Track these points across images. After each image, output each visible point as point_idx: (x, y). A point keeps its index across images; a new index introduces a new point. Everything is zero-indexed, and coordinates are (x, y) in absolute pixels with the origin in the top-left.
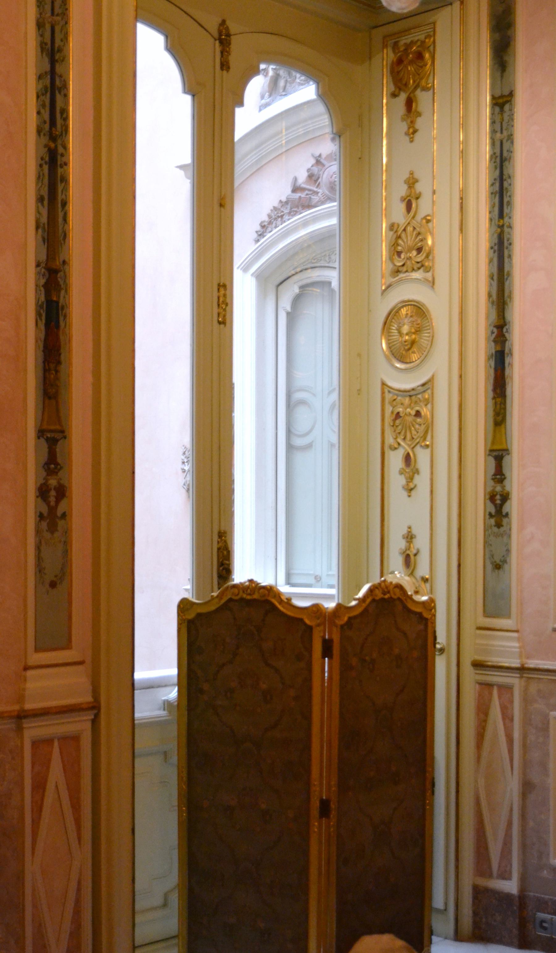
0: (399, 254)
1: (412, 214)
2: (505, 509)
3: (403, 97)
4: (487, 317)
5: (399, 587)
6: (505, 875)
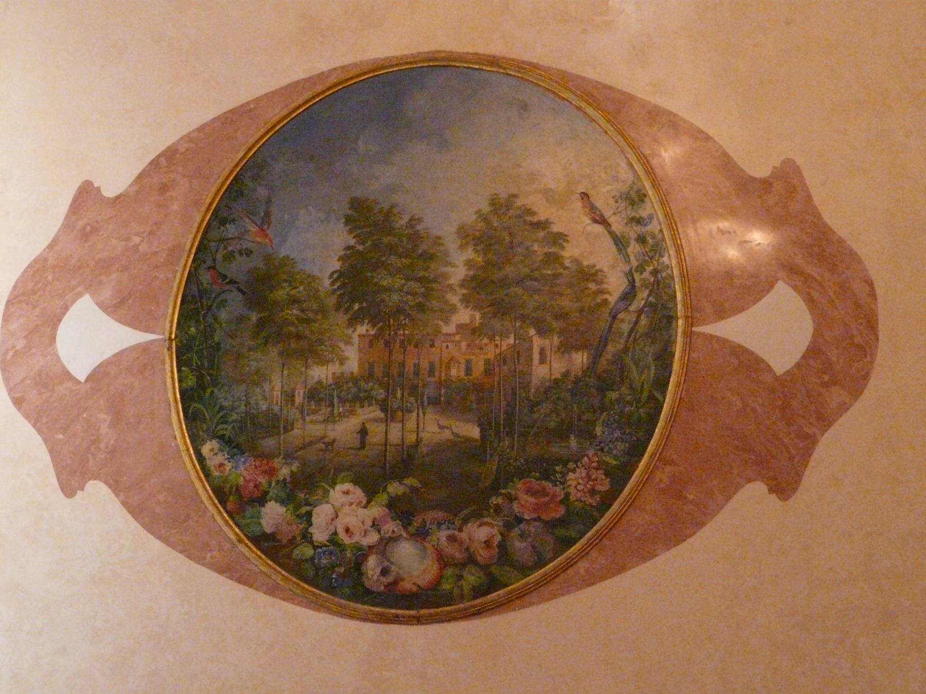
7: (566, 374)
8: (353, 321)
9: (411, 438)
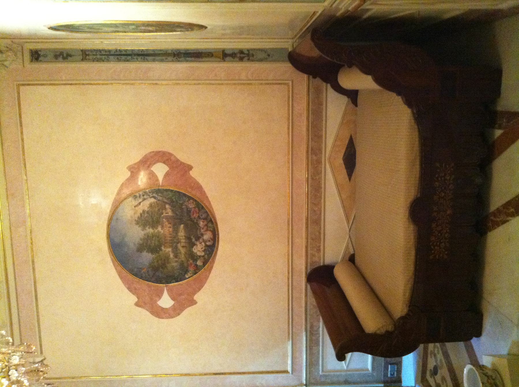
8: (161, 250)
9: (184, 237)
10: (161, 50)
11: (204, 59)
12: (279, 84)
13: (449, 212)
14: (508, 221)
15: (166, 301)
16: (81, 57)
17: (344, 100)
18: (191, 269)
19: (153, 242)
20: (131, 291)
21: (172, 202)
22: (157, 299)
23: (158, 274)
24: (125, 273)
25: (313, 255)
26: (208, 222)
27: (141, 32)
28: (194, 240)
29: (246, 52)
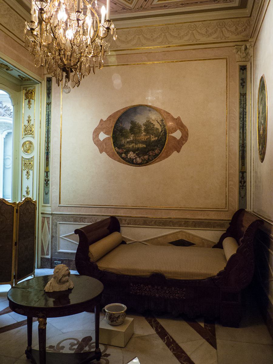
0: (26, 131)
1: (29, 123)
2: (48, 183)
3: (28, 100)
4: (45, 145)
5: (30, 198)
6: (48, 255)
7: (155, 140)
8: (132, 134)
10: (246, 137)
11: (241, 161)
12: (226, 204)
13: (157, 295)
14: (153, 328)
15: (102, 136)
16: (242, 93)
17: (216, 241)
18: (120, 151)
19: (136, 130)
20: (109, 117)
21: (159, 141)
22: (104, 131)
23: (118, 133)
24: (119, 114)
25: (125, 221)
26: (147, 161)
27: (259, 126)
28: (137, 152)
29: (244, 185)
